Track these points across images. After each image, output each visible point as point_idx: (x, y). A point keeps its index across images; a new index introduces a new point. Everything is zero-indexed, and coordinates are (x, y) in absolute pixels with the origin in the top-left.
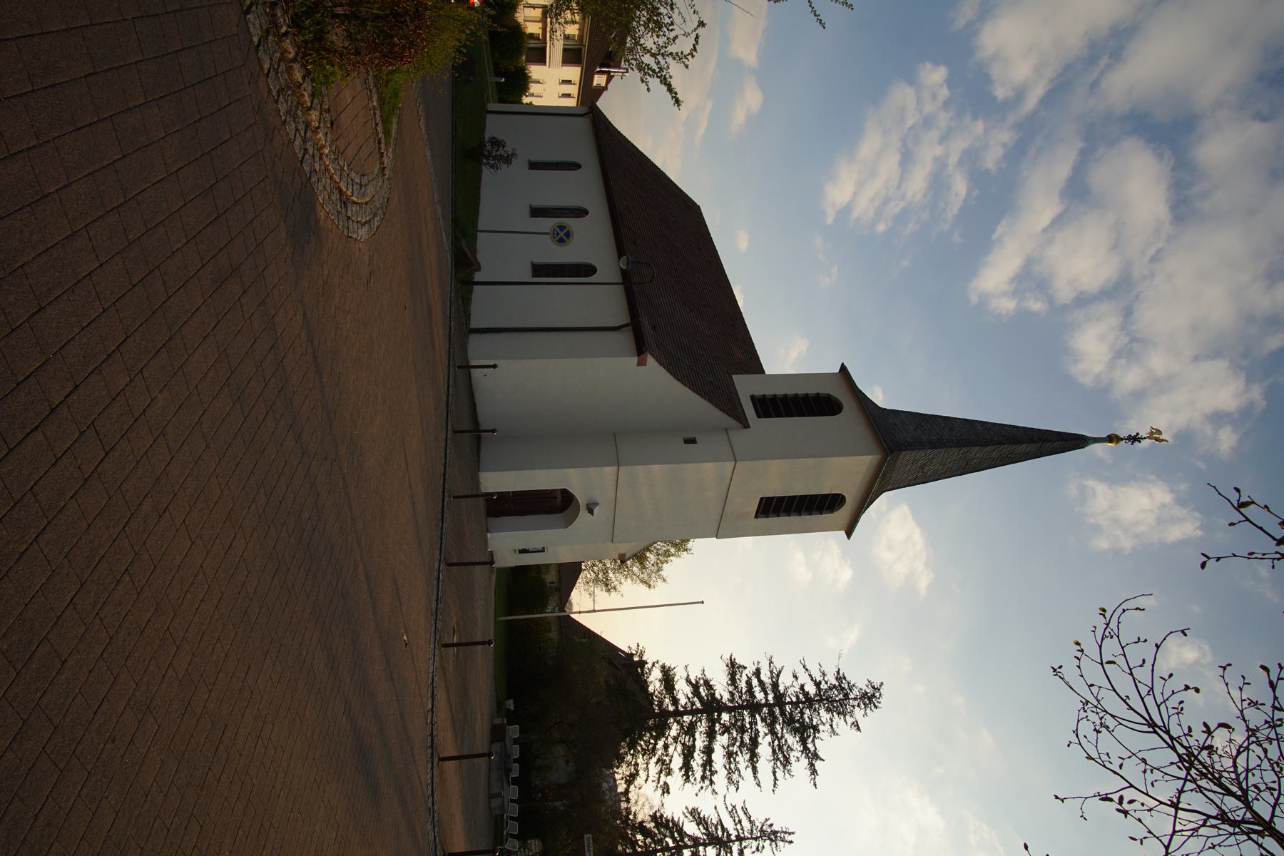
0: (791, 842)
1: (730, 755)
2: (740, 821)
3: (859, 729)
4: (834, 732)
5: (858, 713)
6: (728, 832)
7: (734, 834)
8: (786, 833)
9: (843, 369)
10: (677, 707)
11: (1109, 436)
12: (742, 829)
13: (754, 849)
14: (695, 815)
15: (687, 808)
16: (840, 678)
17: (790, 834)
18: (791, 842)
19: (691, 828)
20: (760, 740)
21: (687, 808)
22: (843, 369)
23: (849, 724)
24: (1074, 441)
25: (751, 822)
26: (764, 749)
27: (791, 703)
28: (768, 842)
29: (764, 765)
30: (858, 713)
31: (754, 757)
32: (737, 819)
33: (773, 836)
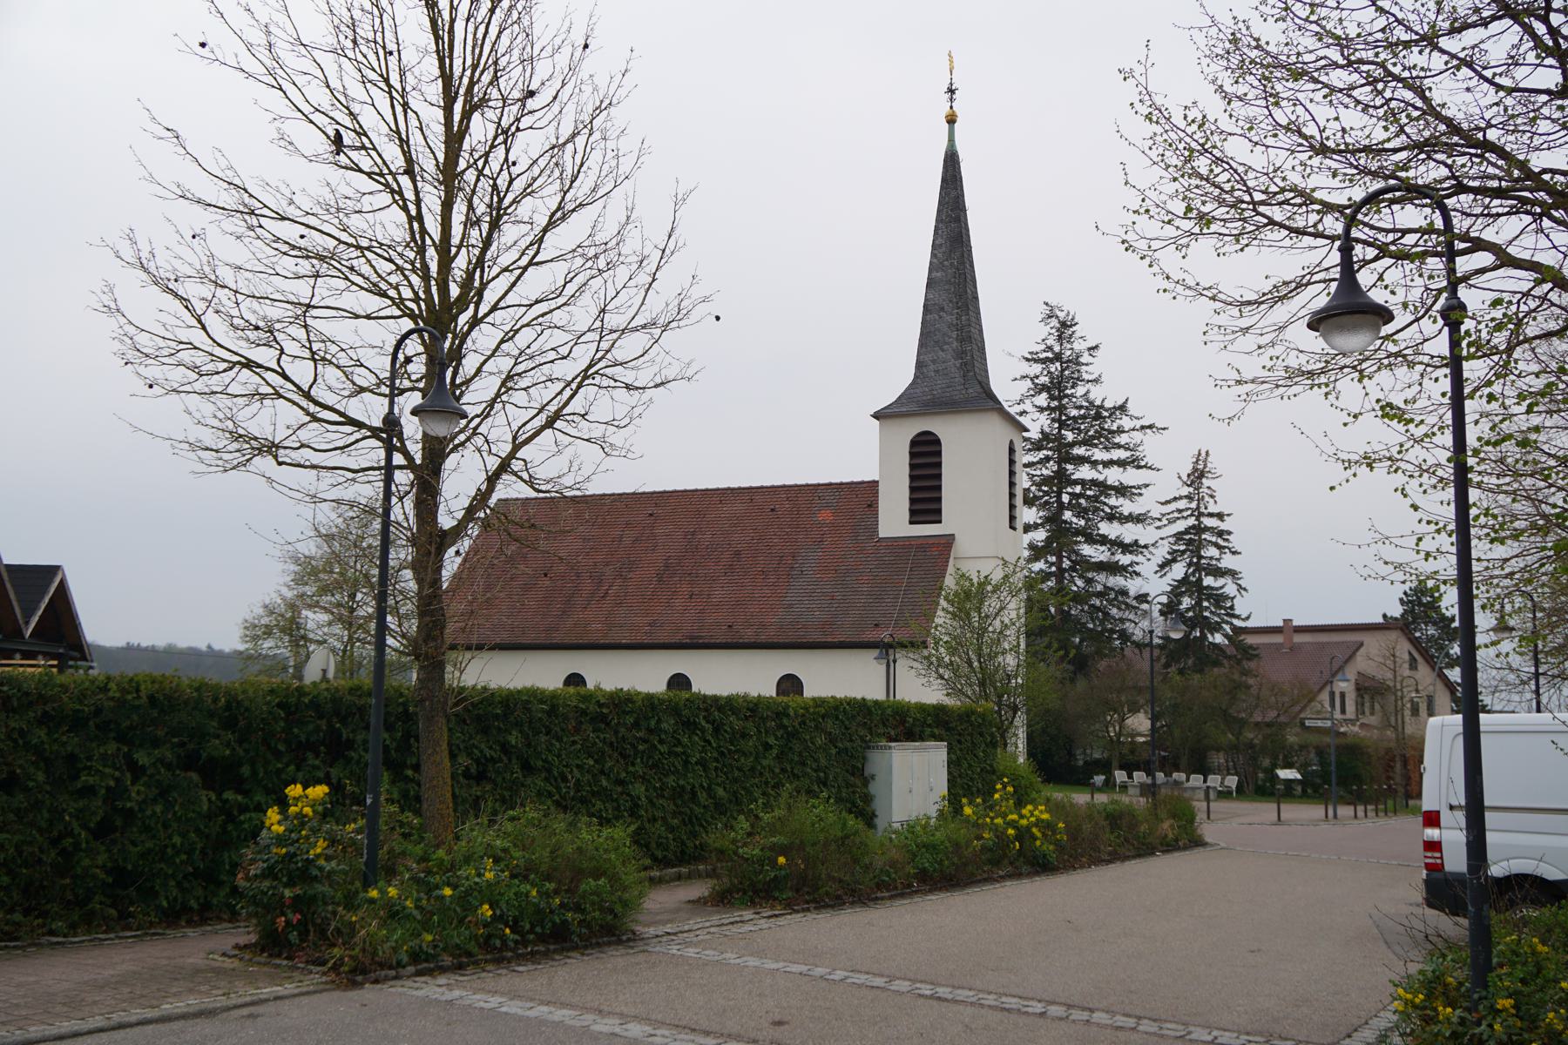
0: (1207, 453)
1: (1111, 518)
2: (1180, 511)
3: (1096, 347)
4: (1096, 381)
5: (1079, 346)
6: (1190, 528)
7: (1192, 521)
8: (1198, 460)
9: (877, 416)
10: (1051, 574)
11: (948, 122)
12: (1187, 509)
13: (1211, 501)
14: (1165, 565)
15: (1156, 572)
16: (1033, 359)
17: (1199, 454)
18: (1207, 453)
19: (1178, 571)
20: (1101, 478)
21: (1156, 572)
22: (877, 416)
23: (1090, 359)
24: (952, 162)
25: (1181, 498)
26: (1113, 476)
27: (1060, 428)
28: (1204, 480)
29: (1130, 477)
30: (1079, 346)
31: (1122, 491)
32: (1176, 515)
33: (1198, 475)
